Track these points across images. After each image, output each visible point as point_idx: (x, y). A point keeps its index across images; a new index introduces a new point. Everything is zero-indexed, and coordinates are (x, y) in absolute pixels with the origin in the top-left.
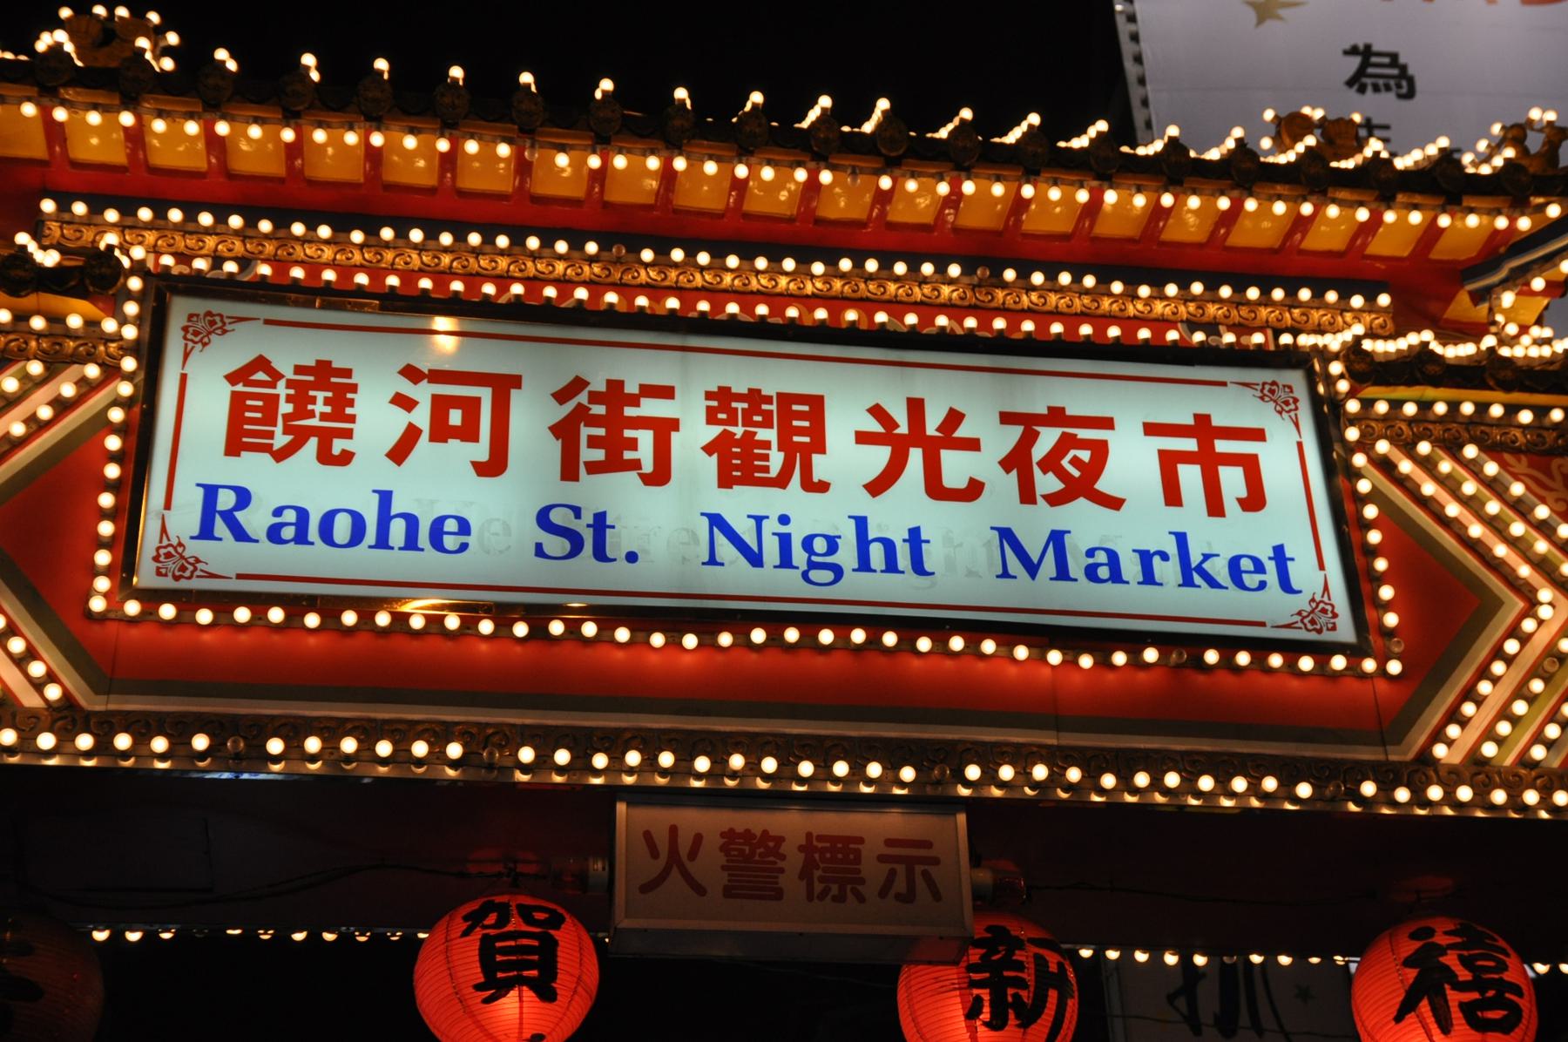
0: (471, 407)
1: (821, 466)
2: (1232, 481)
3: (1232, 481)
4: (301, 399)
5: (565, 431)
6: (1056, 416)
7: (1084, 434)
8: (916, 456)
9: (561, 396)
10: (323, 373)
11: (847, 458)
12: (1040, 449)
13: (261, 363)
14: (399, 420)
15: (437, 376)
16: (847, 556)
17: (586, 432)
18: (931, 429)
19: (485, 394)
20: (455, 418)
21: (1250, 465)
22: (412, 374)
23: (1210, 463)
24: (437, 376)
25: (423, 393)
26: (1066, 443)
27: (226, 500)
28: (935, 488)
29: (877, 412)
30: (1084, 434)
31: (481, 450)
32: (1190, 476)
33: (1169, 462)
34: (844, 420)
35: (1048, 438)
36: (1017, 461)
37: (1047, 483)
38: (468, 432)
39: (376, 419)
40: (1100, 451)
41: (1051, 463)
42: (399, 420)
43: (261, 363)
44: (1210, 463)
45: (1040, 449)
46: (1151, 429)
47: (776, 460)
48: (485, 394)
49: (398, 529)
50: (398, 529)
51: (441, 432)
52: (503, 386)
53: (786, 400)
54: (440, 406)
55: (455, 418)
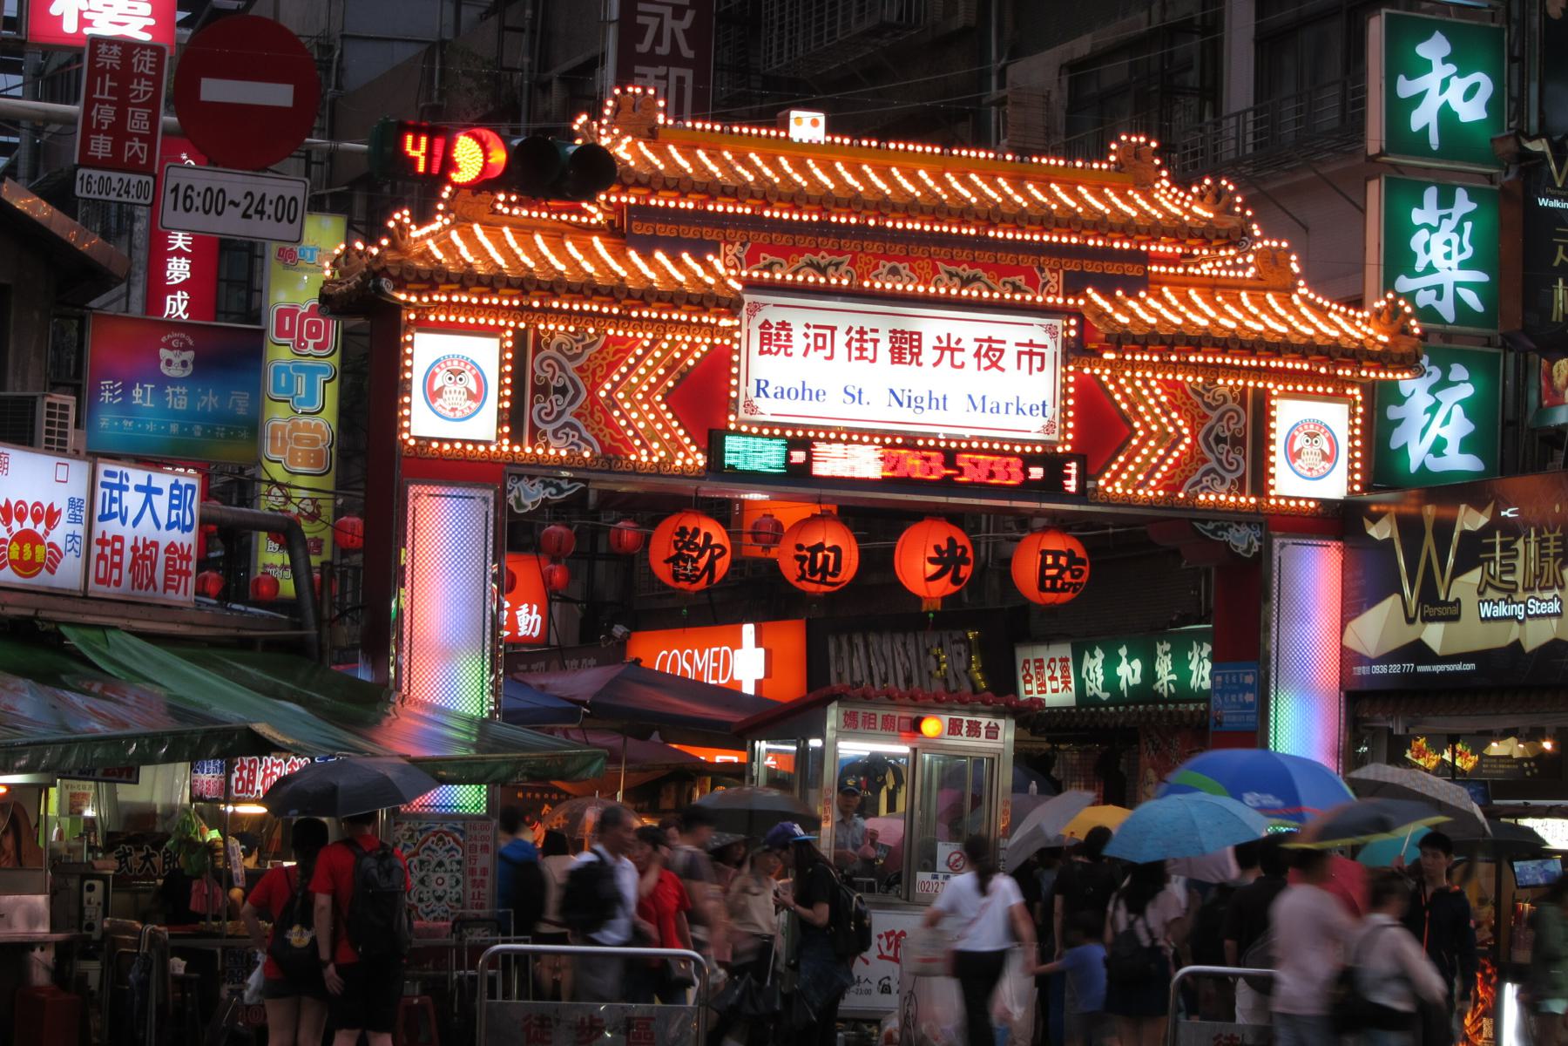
0: (824, 336)
1: (921, 359)
2: (1037, 360)
3: (1037, 360)
4: (778, 335)
5: (849, 344)
6: (990, 340)
7: (995, 346)
8: (947, 354)
9: (848, 332)
10: (784, 325)
11: (929, 355)
12: (983, 351)
13: (767, 322)
14: (806, 341)
15: (816, 327)
16: (925, 405)
17: (855, 345)
18: (953, 345)
19: (828, 332)
20: (820, 340)
21: (1042, 355)
22: (808, 326)
23: (1031, 354)
24: (816, 327)
25: (812, 332)
26: (990, 348)
27: (763, 385)
28: (953, 365)
29: (939, 339)
30: (995, 346)
31: (827, 352)
32: (1025, 358)
33: (1020, 353)
34: (928, 342)
35: (986, 345)
36: (977, 354)
37: (985, 362)
38: (824, 347)
39: (799, 342)
40: (1002, 351)
41: (986, 355)
42: (806, 341)
43: (767, 322)
44: (1031, 354)
45: (983, 351)
46: (1018, 344)
47: (908, 357)
48: (828, 332)
49: (807, 393)
50: (807, 393)
51: (817, 348)
52: (833, 329)
53: (912, 333)
54: (816, 335)
55: (820, 342)
